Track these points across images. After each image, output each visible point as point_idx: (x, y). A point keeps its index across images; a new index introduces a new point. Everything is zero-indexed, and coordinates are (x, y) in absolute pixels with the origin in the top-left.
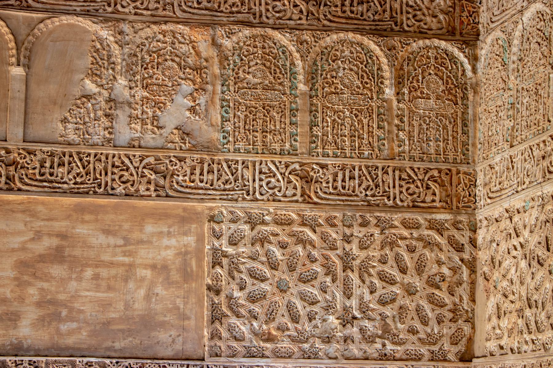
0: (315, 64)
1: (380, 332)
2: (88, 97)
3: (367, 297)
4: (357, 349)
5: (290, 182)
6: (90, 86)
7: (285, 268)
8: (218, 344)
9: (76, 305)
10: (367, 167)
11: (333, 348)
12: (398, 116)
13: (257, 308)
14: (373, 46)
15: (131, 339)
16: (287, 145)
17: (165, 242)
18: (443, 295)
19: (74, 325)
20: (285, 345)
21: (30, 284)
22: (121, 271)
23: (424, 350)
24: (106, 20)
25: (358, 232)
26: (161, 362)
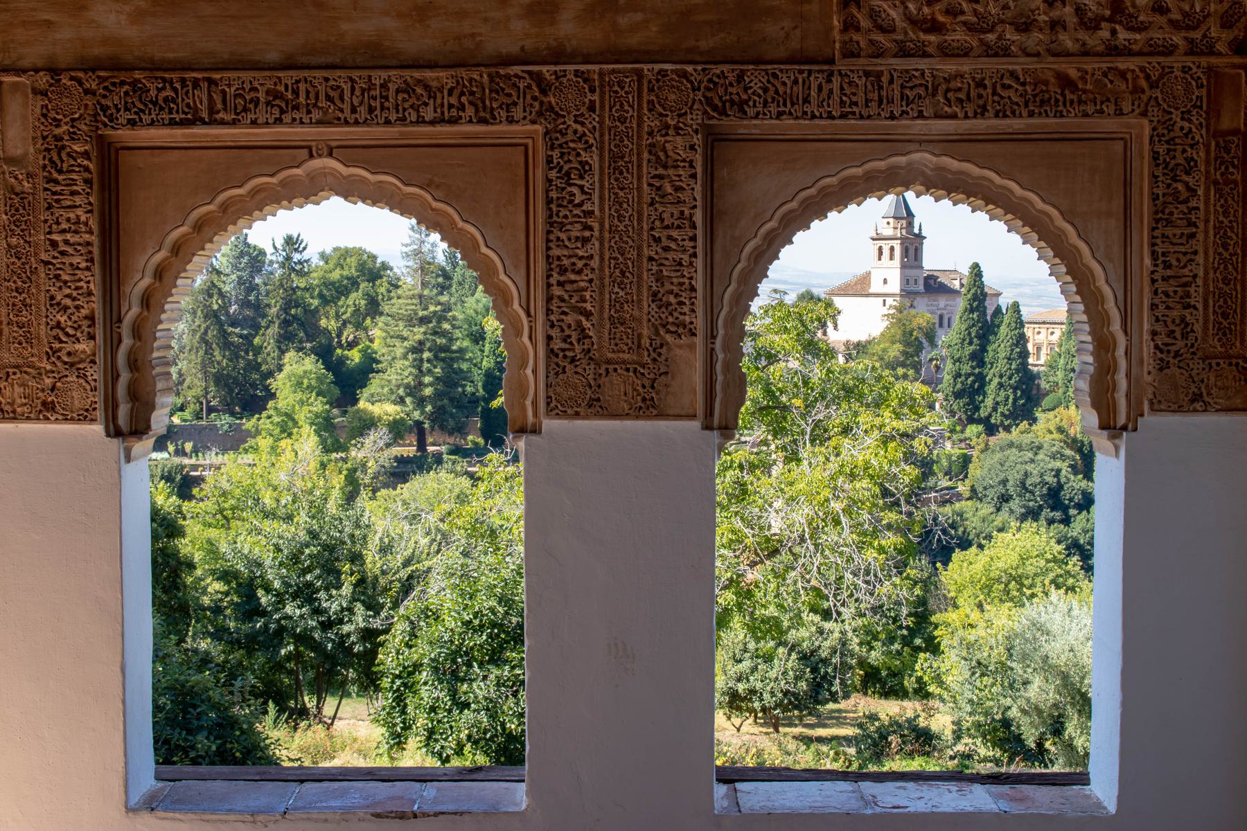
1: (1108, 13)
4: (1070, 39)
8: (855, 38)
11: (1035, 39)
15: (722, 35)
19: (639, 17)
20: (958, 36)
23: (1177, 39)
26: (769, 67)
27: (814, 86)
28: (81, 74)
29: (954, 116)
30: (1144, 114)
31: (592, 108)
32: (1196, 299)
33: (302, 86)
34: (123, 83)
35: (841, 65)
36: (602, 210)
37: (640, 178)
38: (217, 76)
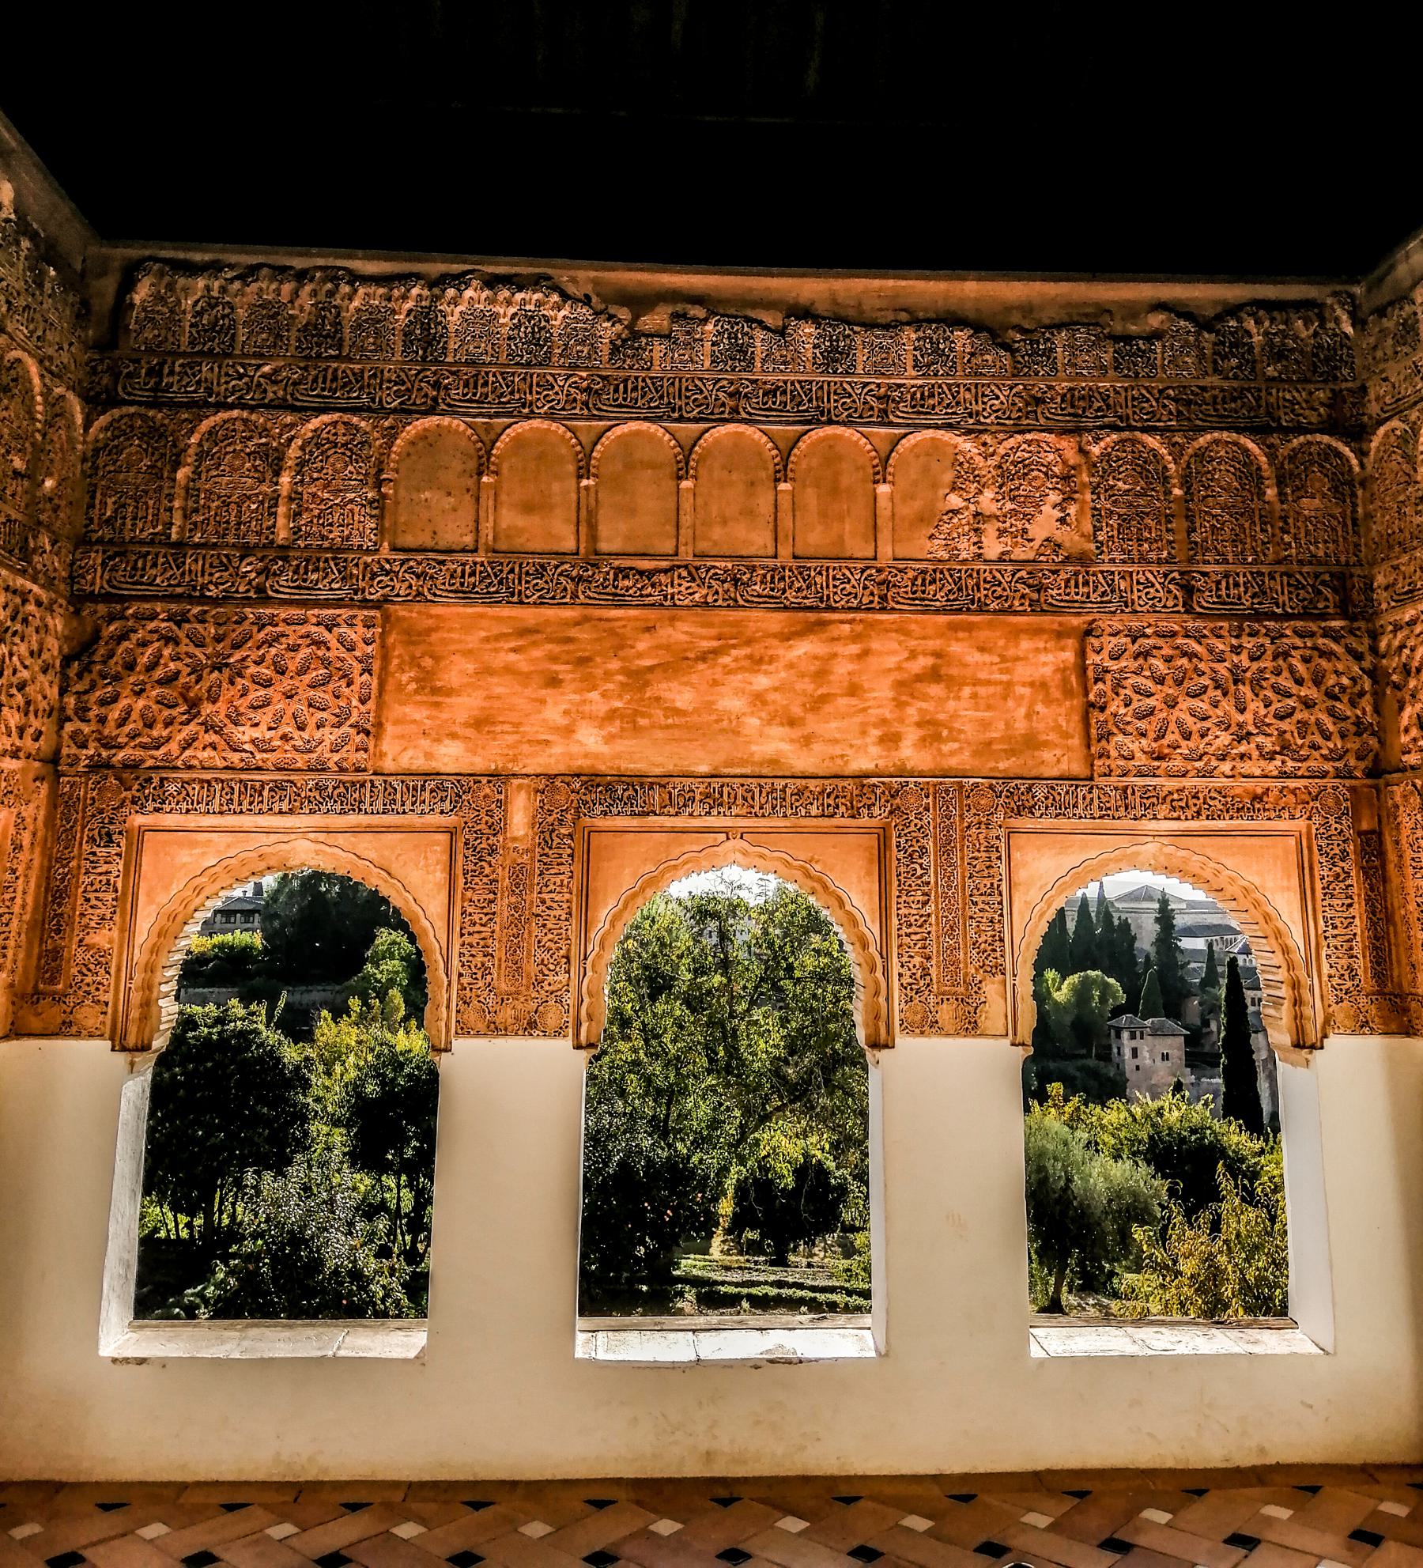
0: (1188, 466)
2: (955, 512)
3: (1263, 711)
5: (1169, 592)
6: (955, 501)
7: (1171, 682)
9: (956, 725)
10: (1252, 573)
11: (1226, 767)
12: (1281, 517)
13: (1142, 725)
14: (1251, 445)
16: (1165, 554)
17: (1043, 658)
18: (1342, 707)
19: (956, 745)
20: (1177, 763)
21: (907, 704)
22: (999, 689)
23: (1328, 767)
24: (969, 432)
25: (1248, 643)
27: (1080, 796)
28: (568, 779)
29: (1178, 819)
30: (1309, 818)
31: (927, 809)
32: (1357, 951)
33: (726, 790)
34: (598, 785)
35: (1100, 781)
36: (936, 883)
37: (962, 858)
38: (664, 781)
